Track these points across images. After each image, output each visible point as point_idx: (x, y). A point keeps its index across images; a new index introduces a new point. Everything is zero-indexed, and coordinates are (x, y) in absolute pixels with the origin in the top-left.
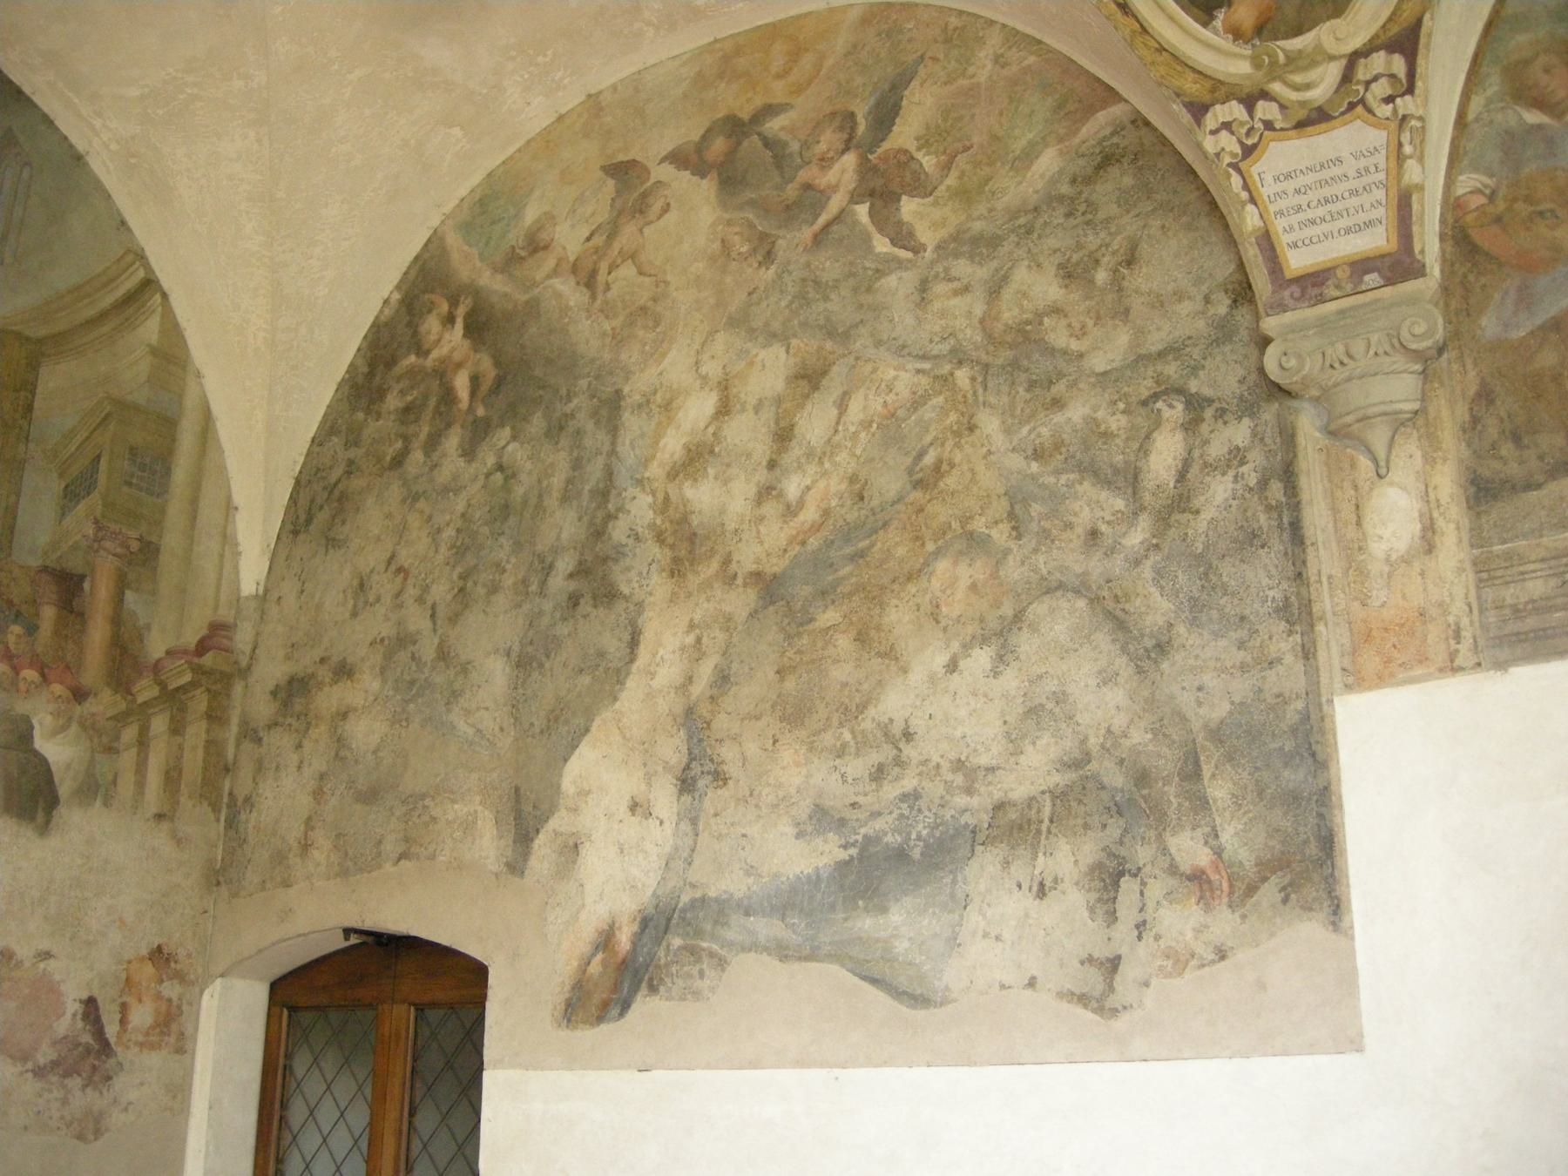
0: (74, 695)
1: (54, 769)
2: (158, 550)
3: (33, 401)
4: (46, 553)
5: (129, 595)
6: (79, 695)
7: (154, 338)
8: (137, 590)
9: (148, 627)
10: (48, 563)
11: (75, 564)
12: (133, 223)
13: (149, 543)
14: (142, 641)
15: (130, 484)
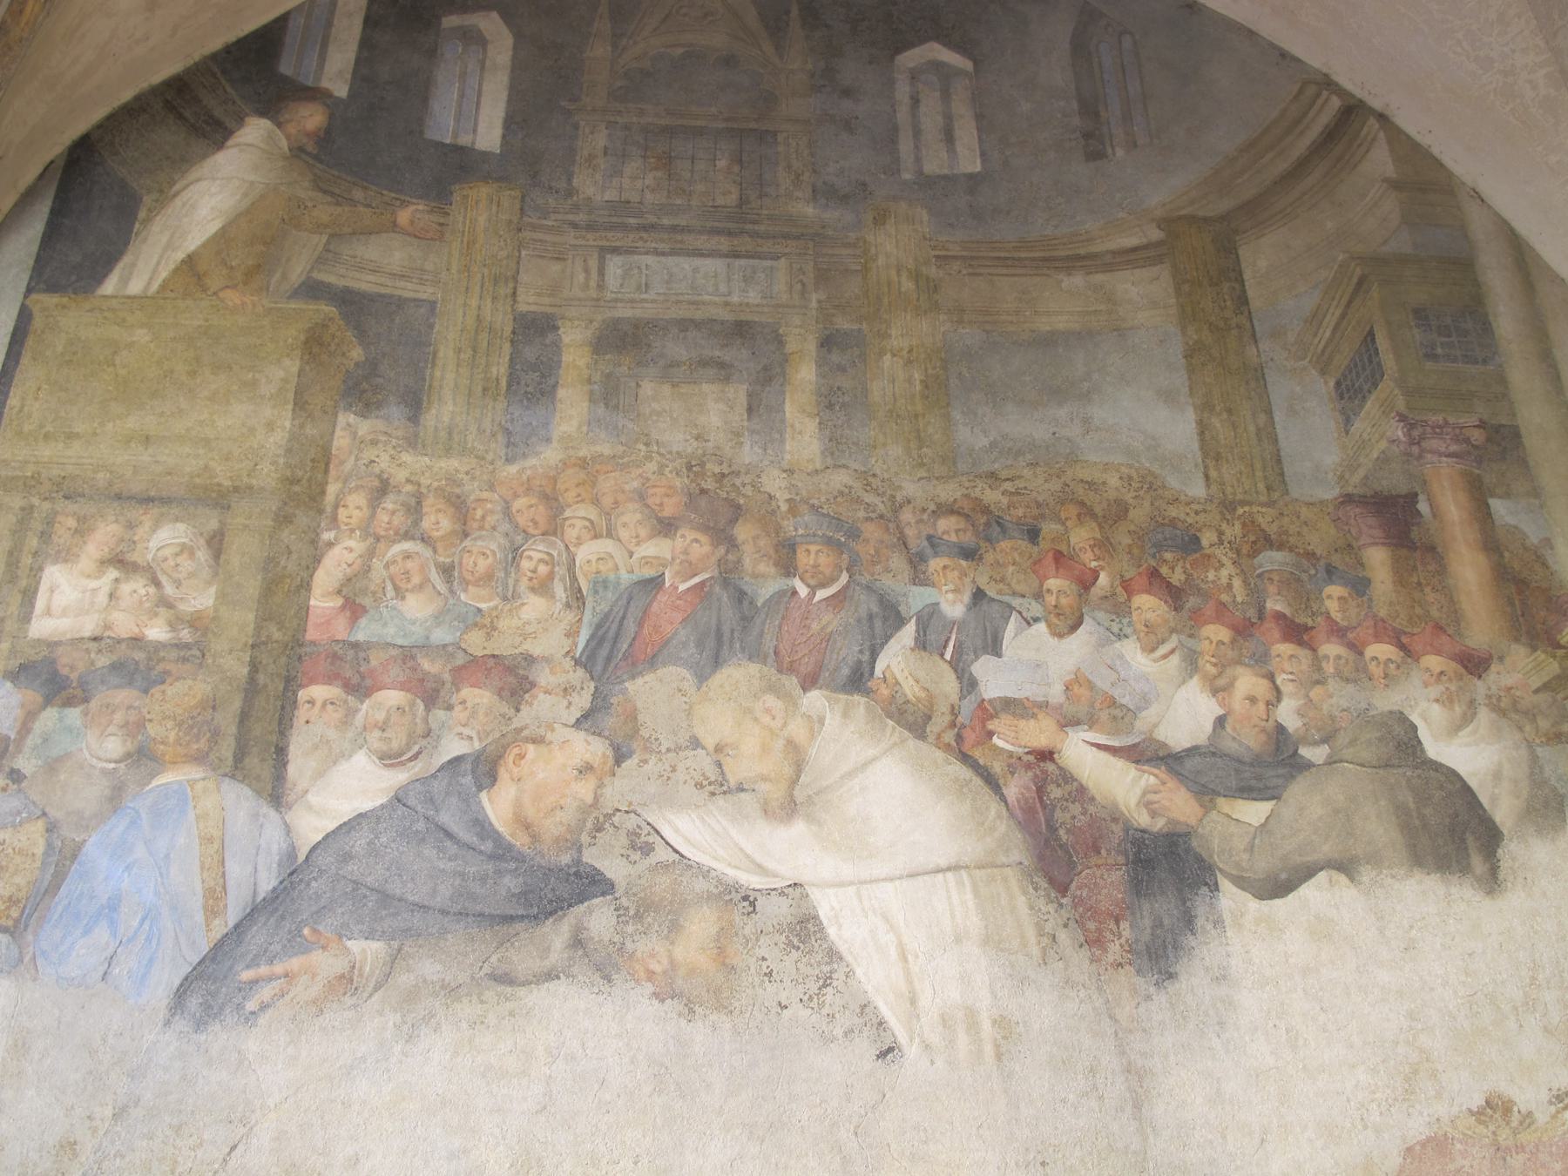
0: (1466, 667)
1: (1473, 783)
2: (1516, 435)
3: (1244, 292)
4: (1341, 477)
5: (1497, 505)
6: (1474, 664)
7: (1390, 170)
8: (1507, 495)
9: (1548, 542)
10: (1350, 490)
11: (1394, 482)
12: (1296, 50)
13: (1498, 429)
14: (1545, 565)
15: (1431, 356)
